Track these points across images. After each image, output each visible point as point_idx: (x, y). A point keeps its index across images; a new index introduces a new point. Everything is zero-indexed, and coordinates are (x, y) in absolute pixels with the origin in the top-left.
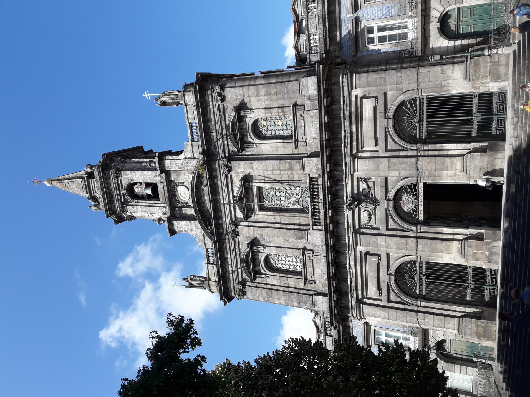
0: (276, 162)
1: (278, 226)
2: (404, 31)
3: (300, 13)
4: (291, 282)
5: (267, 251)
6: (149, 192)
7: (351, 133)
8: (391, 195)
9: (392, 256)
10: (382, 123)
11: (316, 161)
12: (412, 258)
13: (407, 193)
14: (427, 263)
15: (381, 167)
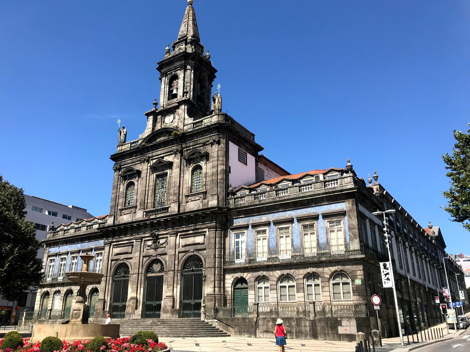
0: (178, 184)
1: (147, 189)
2: (240, 257)
3: (261, 188)
4: (121, 201)
5: (136, 183)
6: (175, 92)
7: (188, 231)
8: (159, 257)
9: (132, 261)
10: (191, 249)
11: (176, 210)
12: (131, 273)
13: (161, 267)
14: (128, 280)
15: (171, 250)
